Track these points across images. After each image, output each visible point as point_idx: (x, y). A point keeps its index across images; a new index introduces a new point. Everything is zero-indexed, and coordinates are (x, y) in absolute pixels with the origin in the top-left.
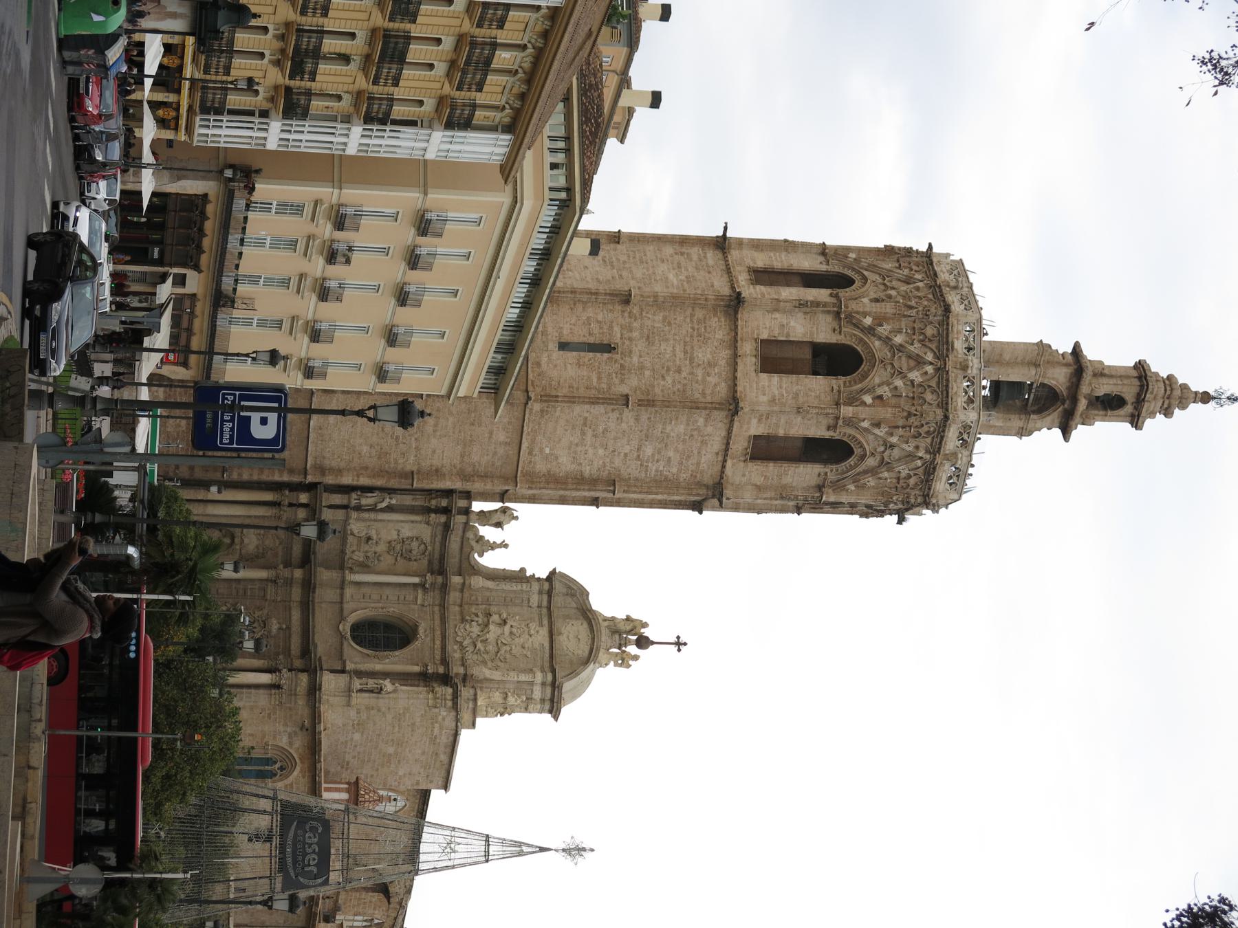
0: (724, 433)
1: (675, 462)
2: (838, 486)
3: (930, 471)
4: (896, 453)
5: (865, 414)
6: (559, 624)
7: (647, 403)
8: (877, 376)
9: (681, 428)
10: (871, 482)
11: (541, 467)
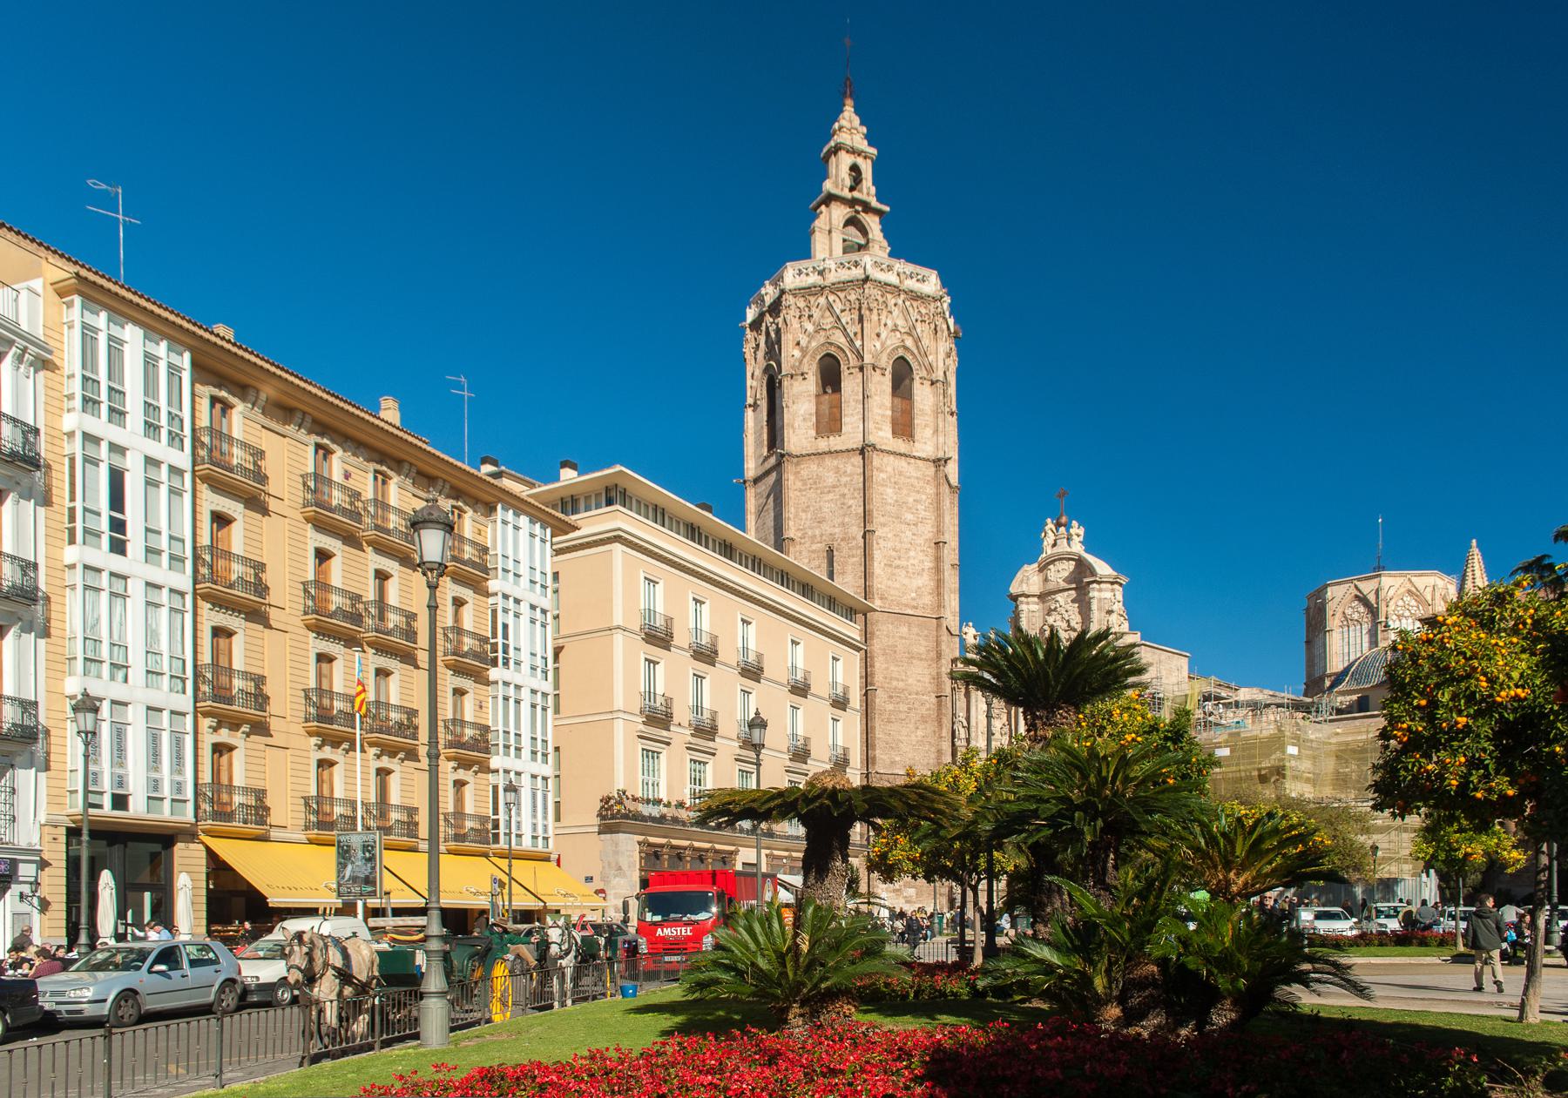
0: (892, 457)
1: (918, 497)
2: (931, 368)
3: (916, 296)
4: (901, 322)
5: (872, 348)
6: (1051, 586)
7: (866, 517)
8: (839, 339)
9: (889, 491)
10: (926, 342)
11: (928, 600)
